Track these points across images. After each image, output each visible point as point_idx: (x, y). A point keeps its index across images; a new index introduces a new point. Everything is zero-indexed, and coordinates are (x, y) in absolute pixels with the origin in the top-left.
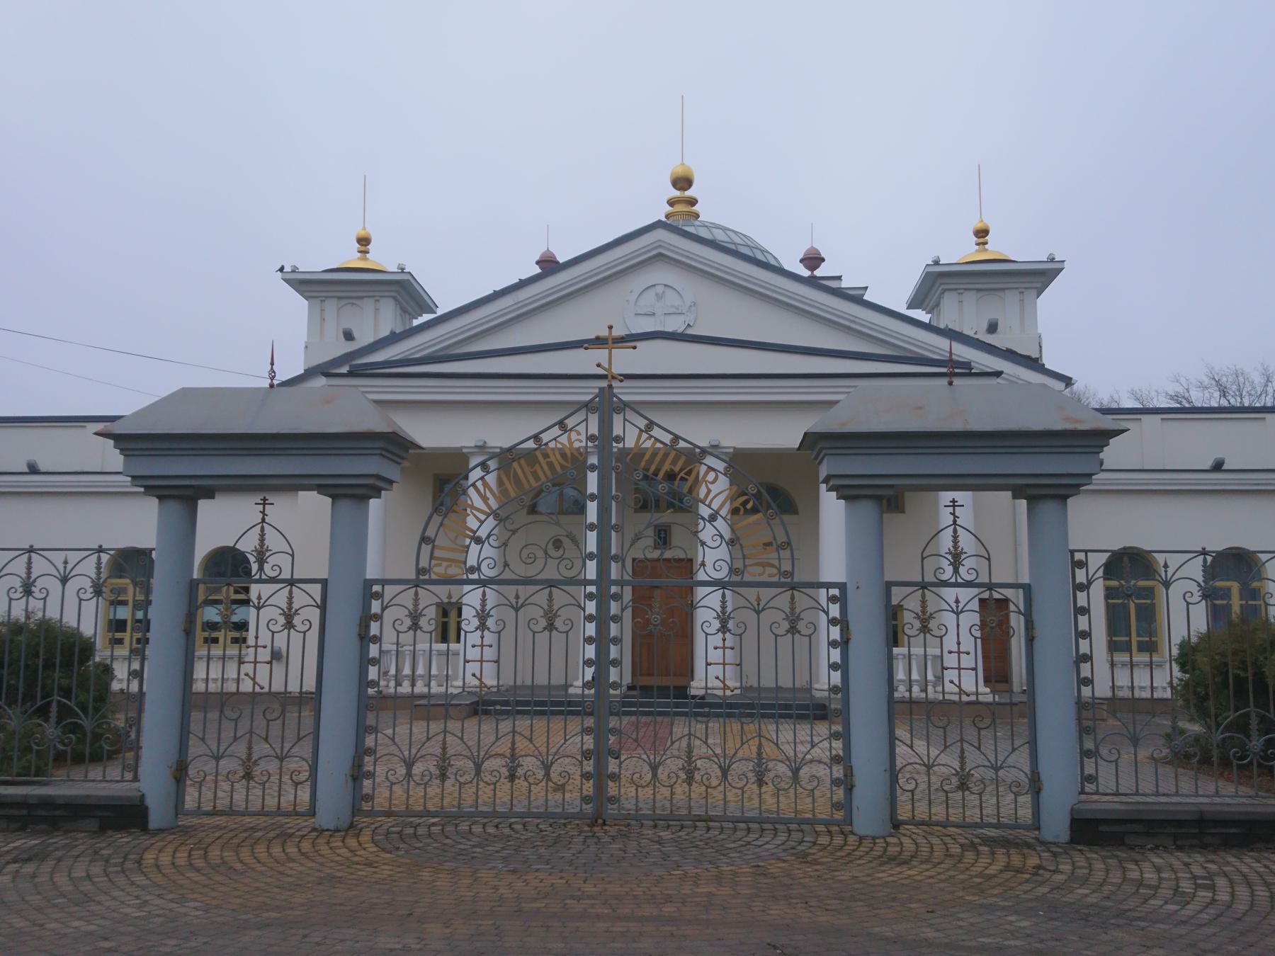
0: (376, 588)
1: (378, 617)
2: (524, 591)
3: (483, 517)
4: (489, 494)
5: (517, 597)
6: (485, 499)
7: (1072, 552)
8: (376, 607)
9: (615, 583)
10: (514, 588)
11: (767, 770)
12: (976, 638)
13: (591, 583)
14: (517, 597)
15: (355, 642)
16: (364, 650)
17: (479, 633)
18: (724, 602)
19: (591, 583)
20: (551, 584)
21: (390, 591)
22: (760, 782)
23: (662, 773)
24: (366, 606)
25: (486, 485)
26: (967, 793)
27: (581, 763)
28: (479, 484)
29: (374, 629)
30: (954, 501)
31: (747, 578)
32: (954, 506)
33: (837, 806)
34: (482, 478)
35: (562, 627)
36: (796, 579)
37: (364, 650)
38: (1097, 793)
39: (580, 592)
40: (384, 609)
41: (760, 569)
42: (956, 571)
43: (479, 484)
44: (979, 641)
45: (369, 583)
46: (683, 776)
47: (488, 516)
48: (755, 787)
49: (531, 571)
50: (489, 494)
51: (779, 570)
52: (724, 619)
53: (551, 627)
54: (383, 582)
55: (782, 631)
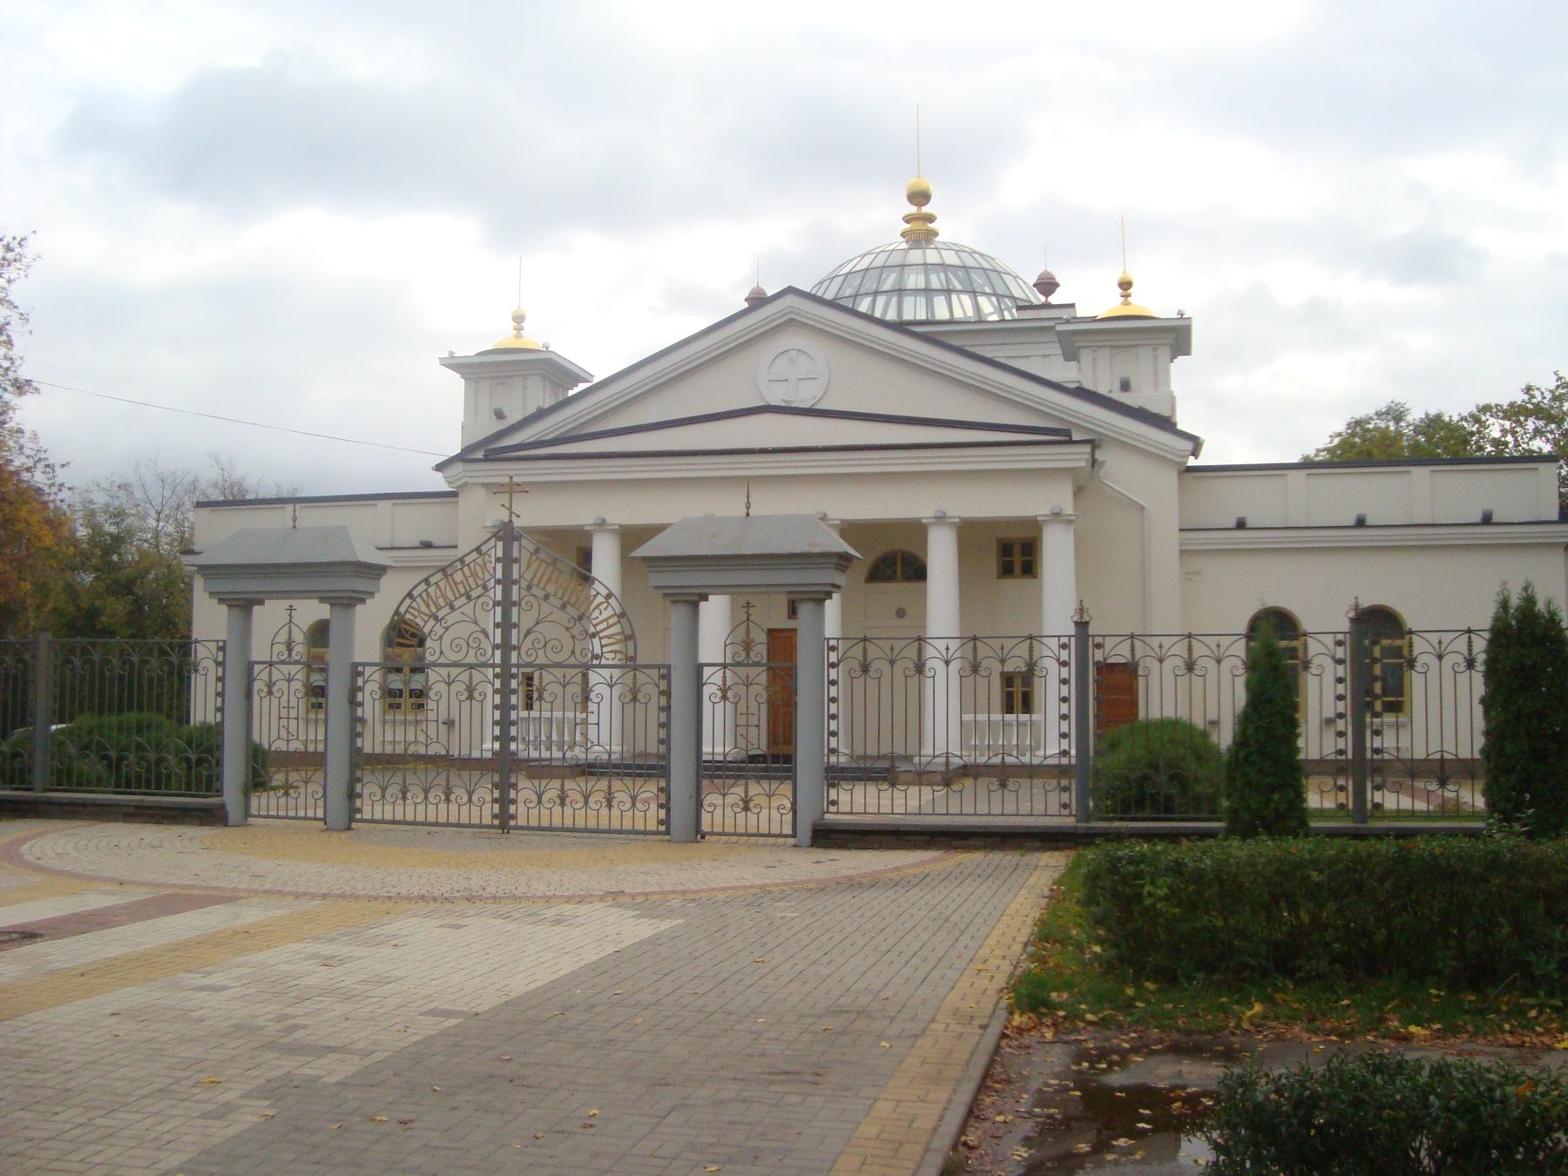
0: (360, 669)
1: (361, 689)
2: (454, 671)
3: (426, 618)
4: (430, 602)
5: (449, 676)
6: (428, 606)
7: (828, 639)
8: (360, 682)
9: (515, 666)
10: (447, 669)
11: (614, 798)
12: (374, 700)
13: (497, 666)
14: (449, 676)
15: (346, 707)
16: (353, 712)
17: (468, 701)
18: (724, 677)
19: (497, 666)
20: (471, 667)
21: (368, 671)
22: (610, 806)
23: (545, 798)
24: (354, 681)
25: (428, 595)
26: (749, 813)
27: (492, 791)
28: (424, 595)
29: (359, 697)
30: (748, 603)
31: (604, 662)
32: (748, 607)
33: (660, 822)
34: (426, 590)
35: (549, 699)
36: (638, 663)
37: (353, 712)
38: (838, 813)
39: (490, 672)
40: (365, 683)
41: (613, 655)
42: (748, 656)
43: (424, 595)
44: (377, 703)
45: (355, 665)
46: (558, 801)
47: (430, 617)
48: (607, 810)
49: (456, 657)
50: (430, 602)
51: (626, 655)
52: (724, 691)
53: (471, 697)
54: (365, 665)
55: (463, 698)
